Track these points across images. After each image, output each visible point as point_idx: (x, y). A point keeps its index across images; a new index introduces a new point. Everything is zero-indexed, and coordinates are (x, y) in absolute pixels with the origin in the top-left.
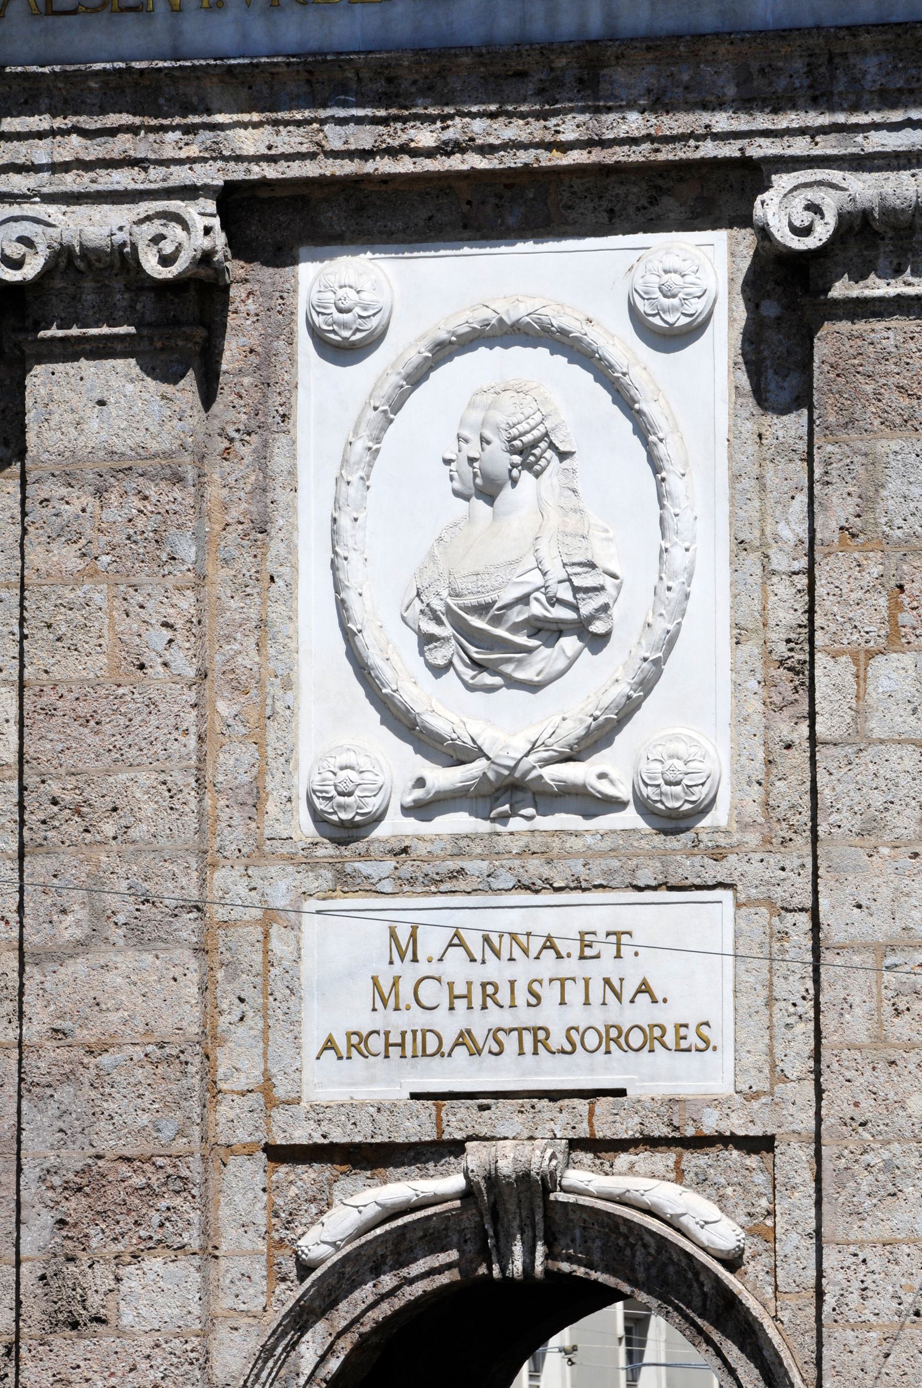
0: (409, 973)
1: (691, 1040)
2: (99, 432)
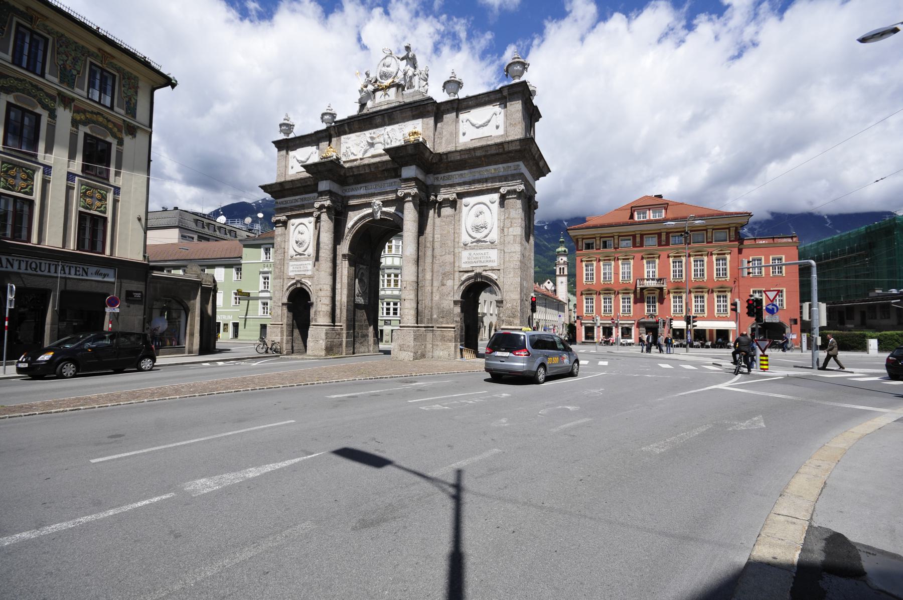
2: (447, 213)
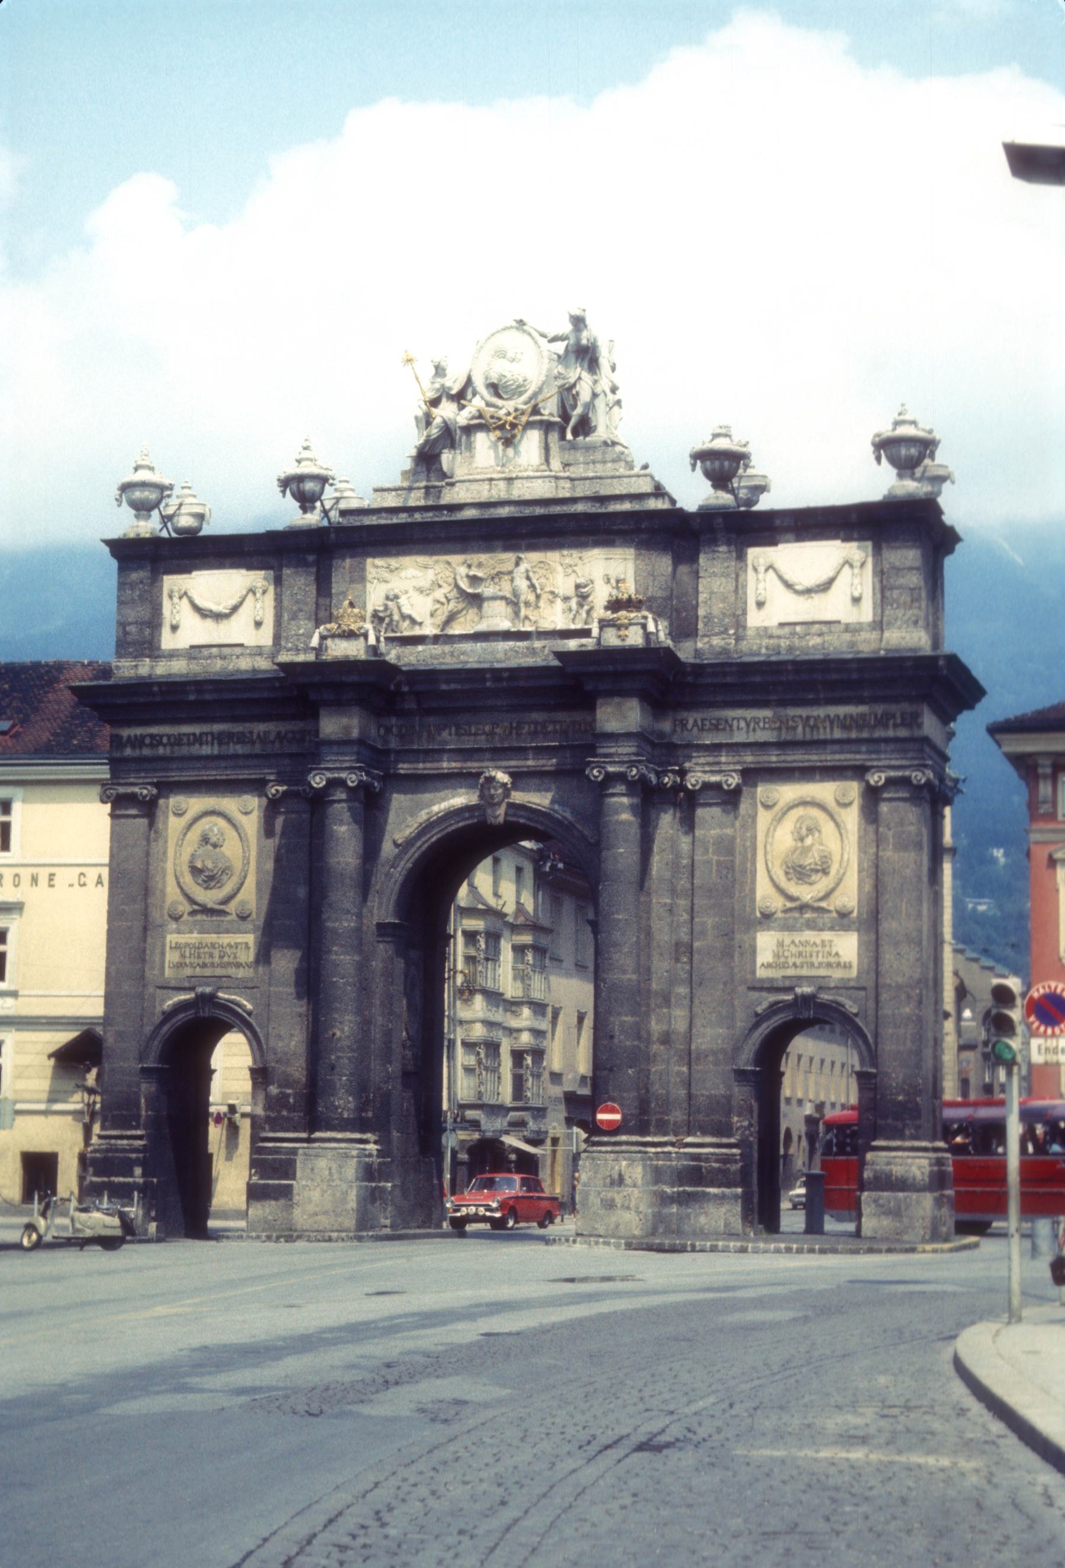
1: (847, 966)
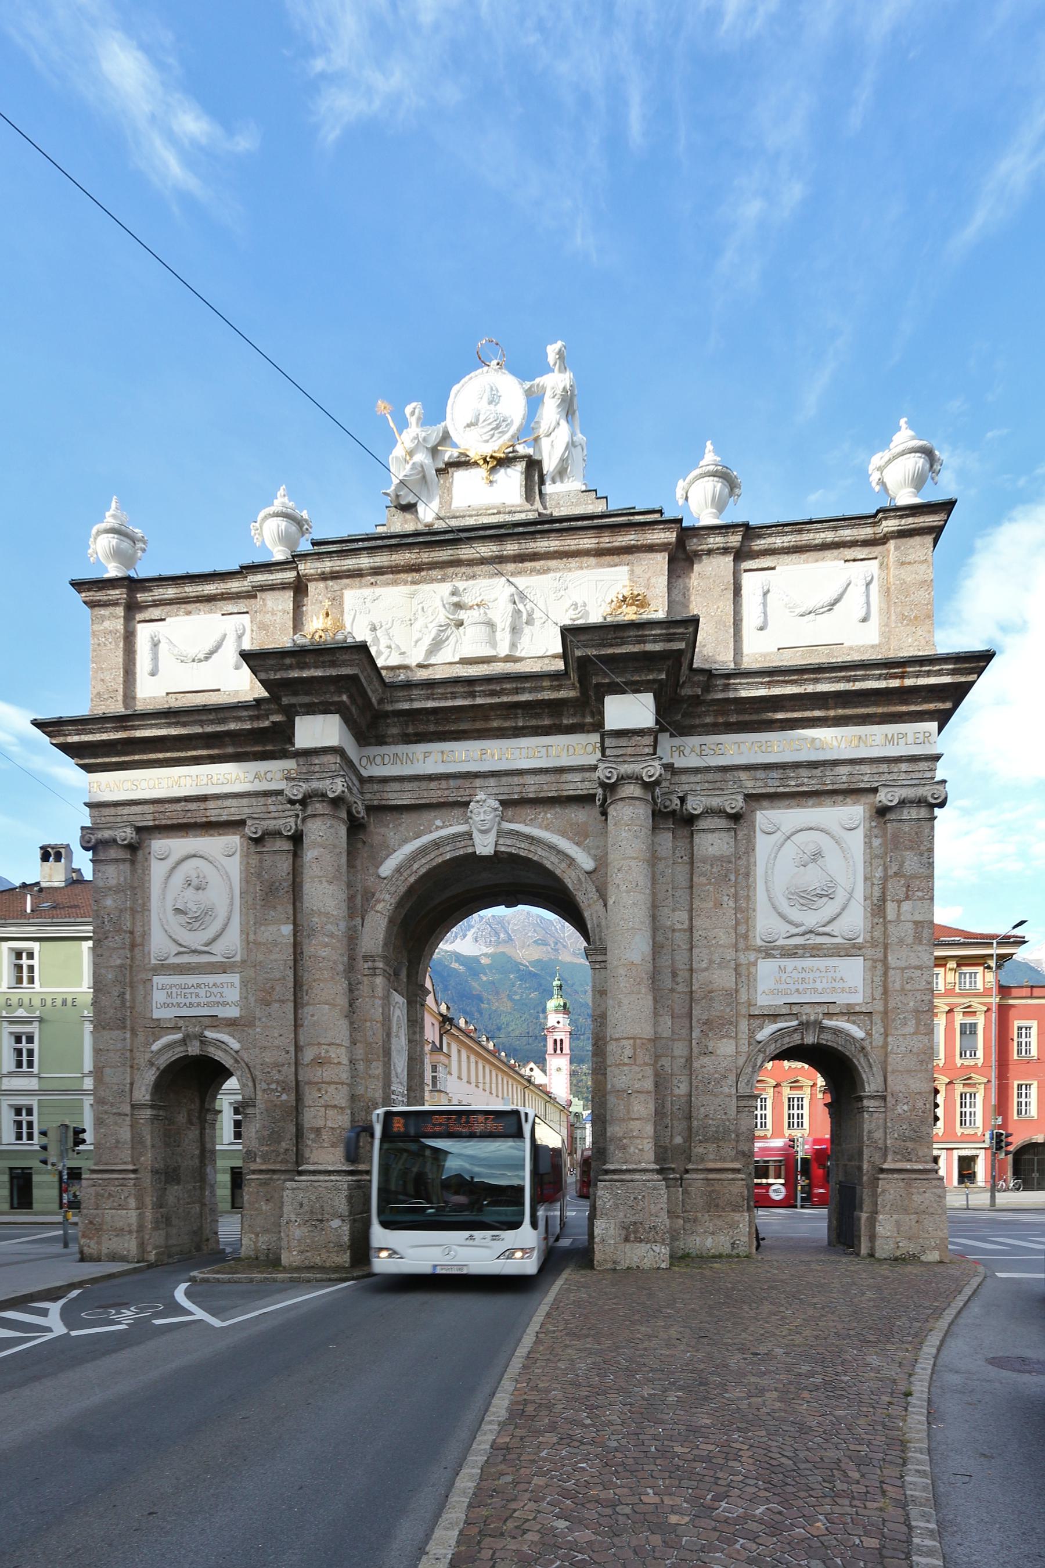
0: (784, 976)
2: (712, 851)
